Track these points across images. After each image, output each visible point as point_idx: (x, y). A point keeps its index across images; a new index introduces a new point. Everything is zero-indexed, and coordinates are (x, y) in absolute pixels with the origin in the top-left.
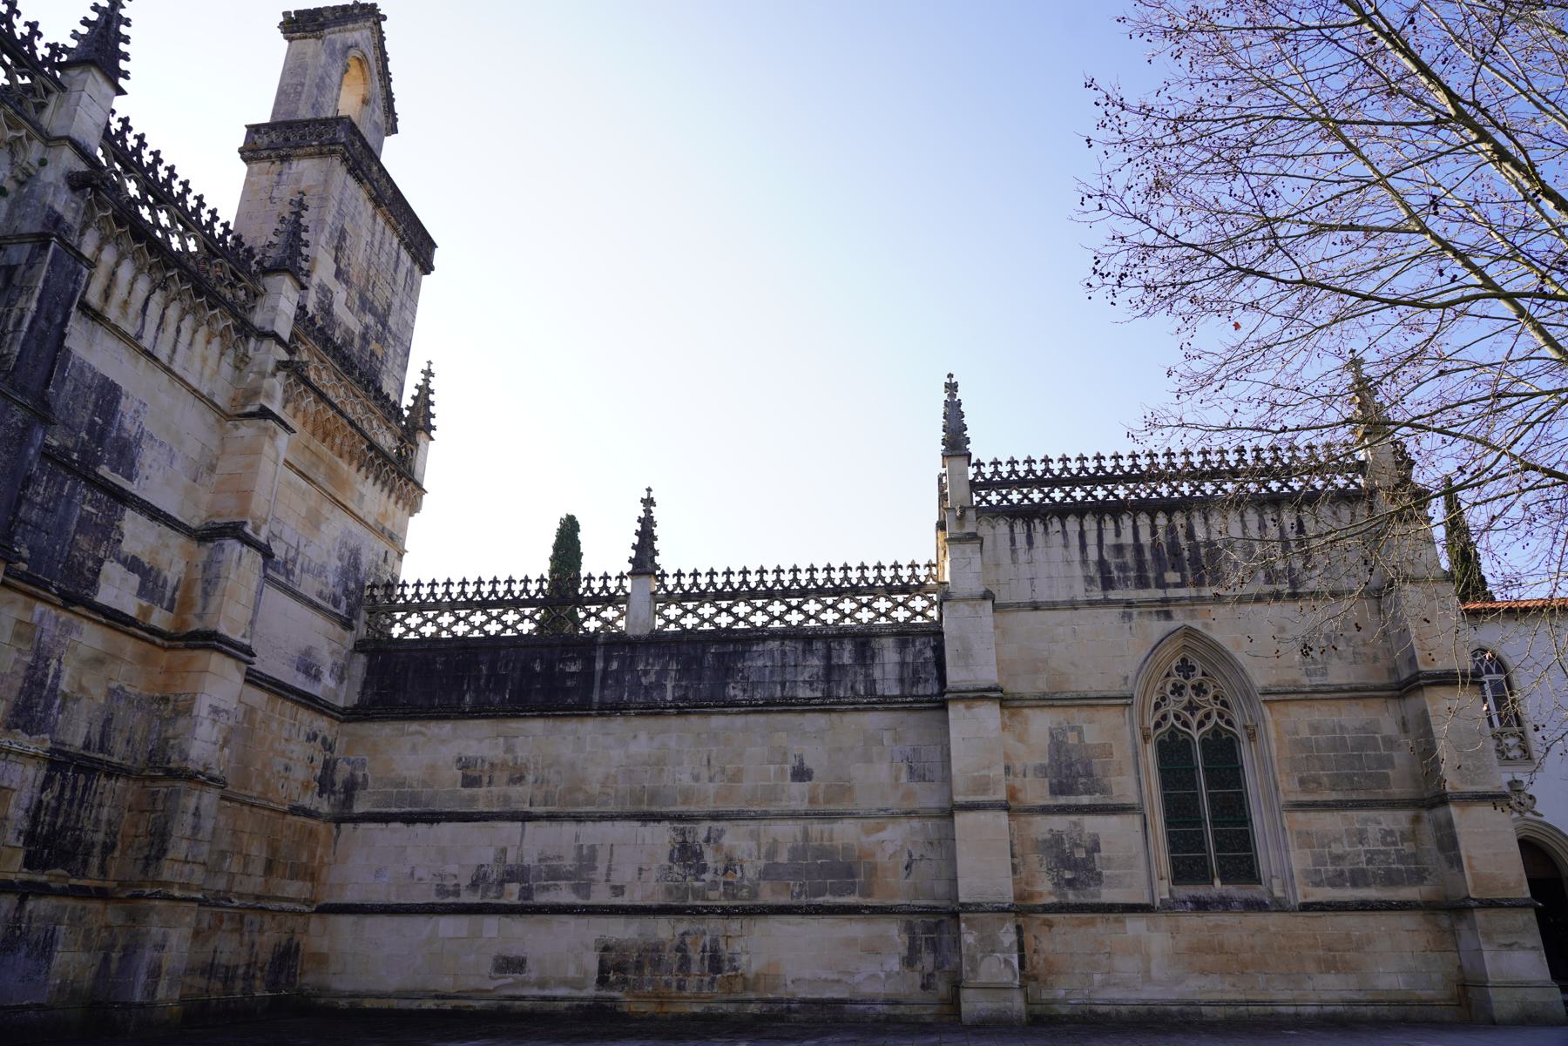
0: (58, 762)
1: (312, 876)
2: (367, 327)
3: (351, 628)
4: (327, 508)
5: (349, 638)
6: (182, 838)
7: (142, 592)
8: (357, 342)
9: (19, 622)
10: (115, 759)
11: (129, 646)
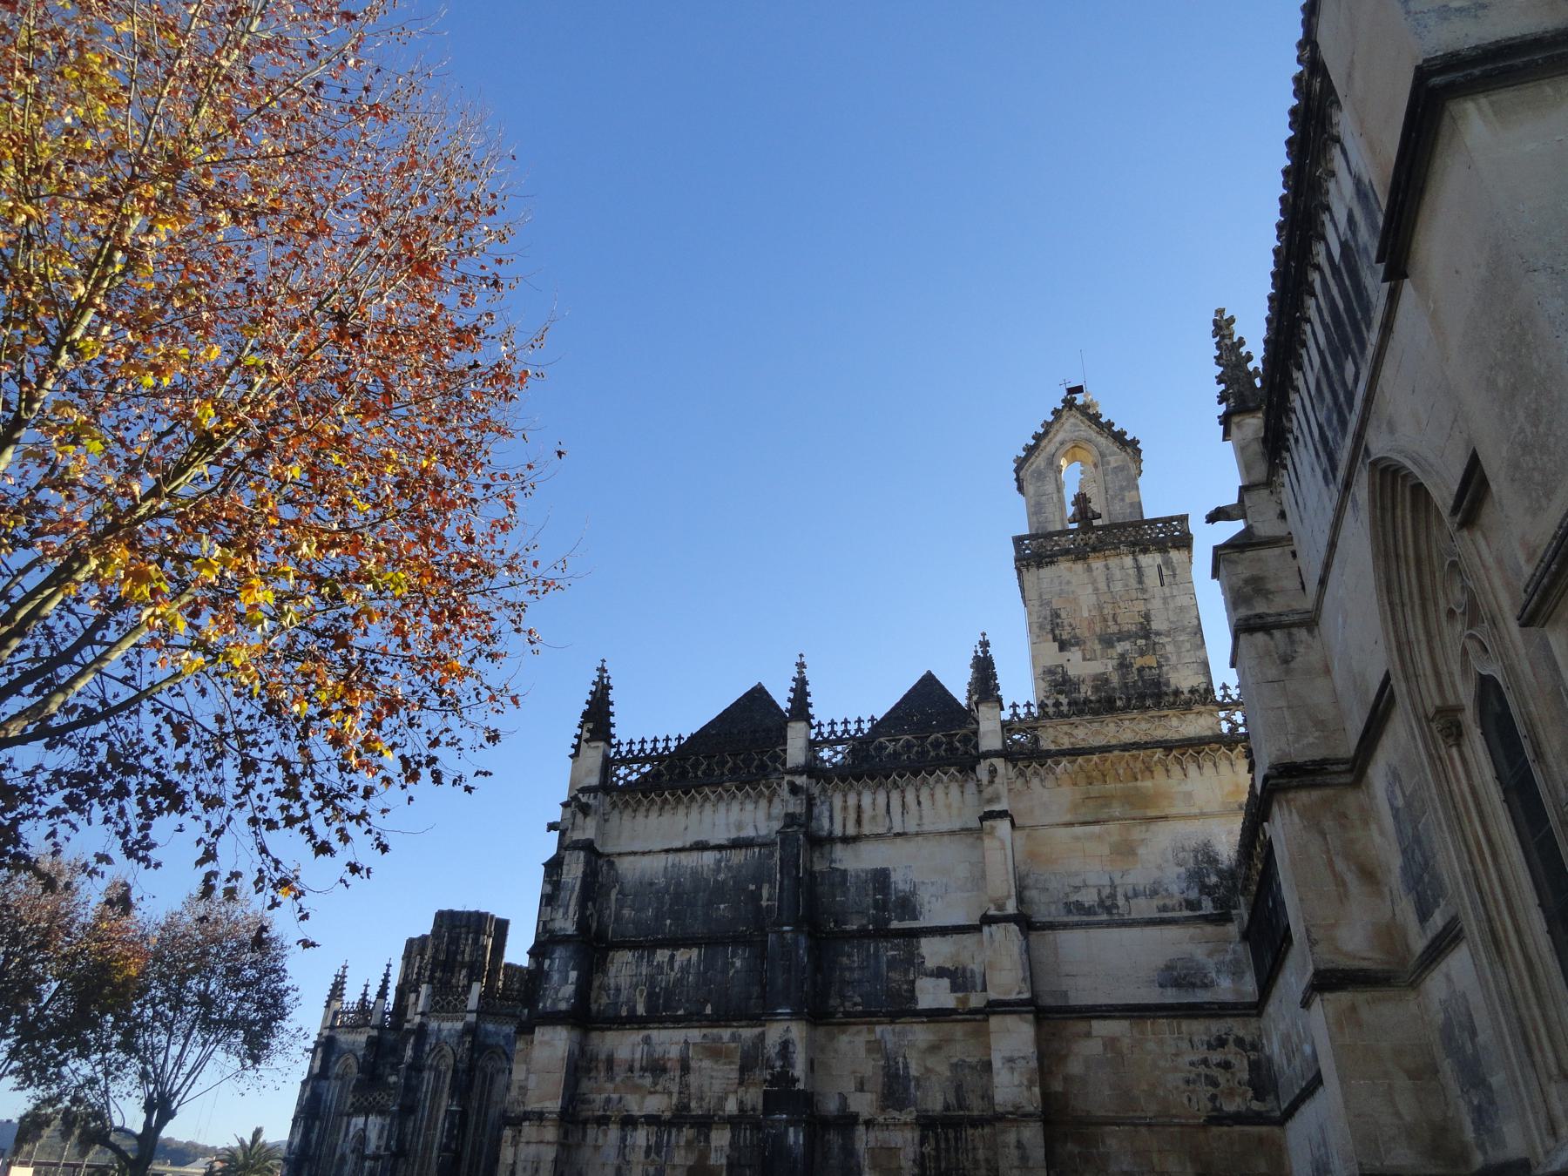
0: (926, 1124)
2: (1122, 656)
3: (1231, 920)
4: (1137, 833)
5: (1233, 929)
7: (955, 988)
8: (1115, 679)
9: (868, 1042)
10: (976, 1113)
11: (959, 1030)
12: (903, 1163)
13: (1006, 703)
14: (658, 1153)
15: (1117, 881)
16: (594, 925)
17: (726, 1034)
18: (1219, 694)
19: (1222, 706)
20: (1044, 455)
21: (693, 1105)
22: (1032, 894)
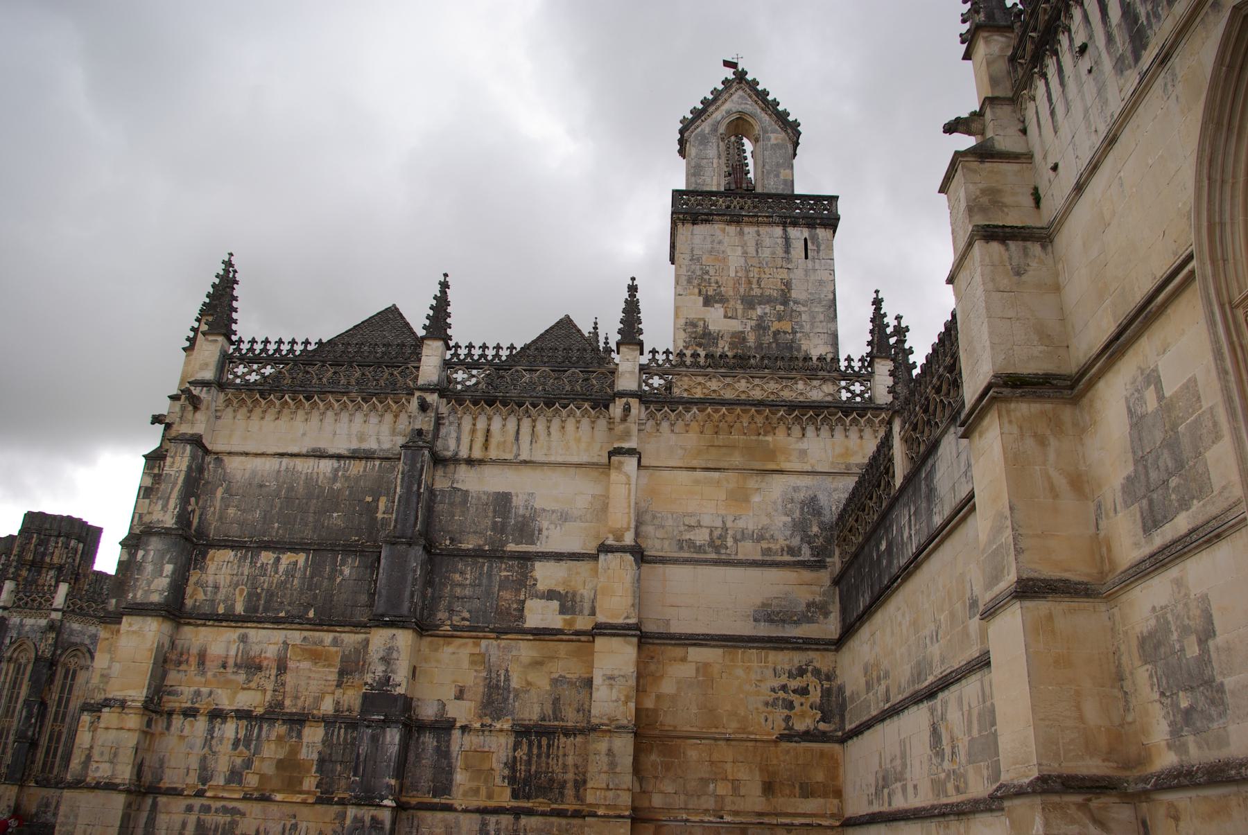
0: (523, 732)
1: (838, 793)
2: (761, 318)
3: (825, 567)
4: (752, 483)
5: (825, 577)
6: (600, 772)
7: (563, 611)
8: (751, 339)
10: (570, 724)
12: (494, 765)
13: (647, 349)
14: (247, 746)
15: (729, 524)
16: (195, 522)
17: (328, 637)
18: (843, 364)
19: (844, 376)
20: (709, 121)
21: (287, 702)
22: (649, 529)
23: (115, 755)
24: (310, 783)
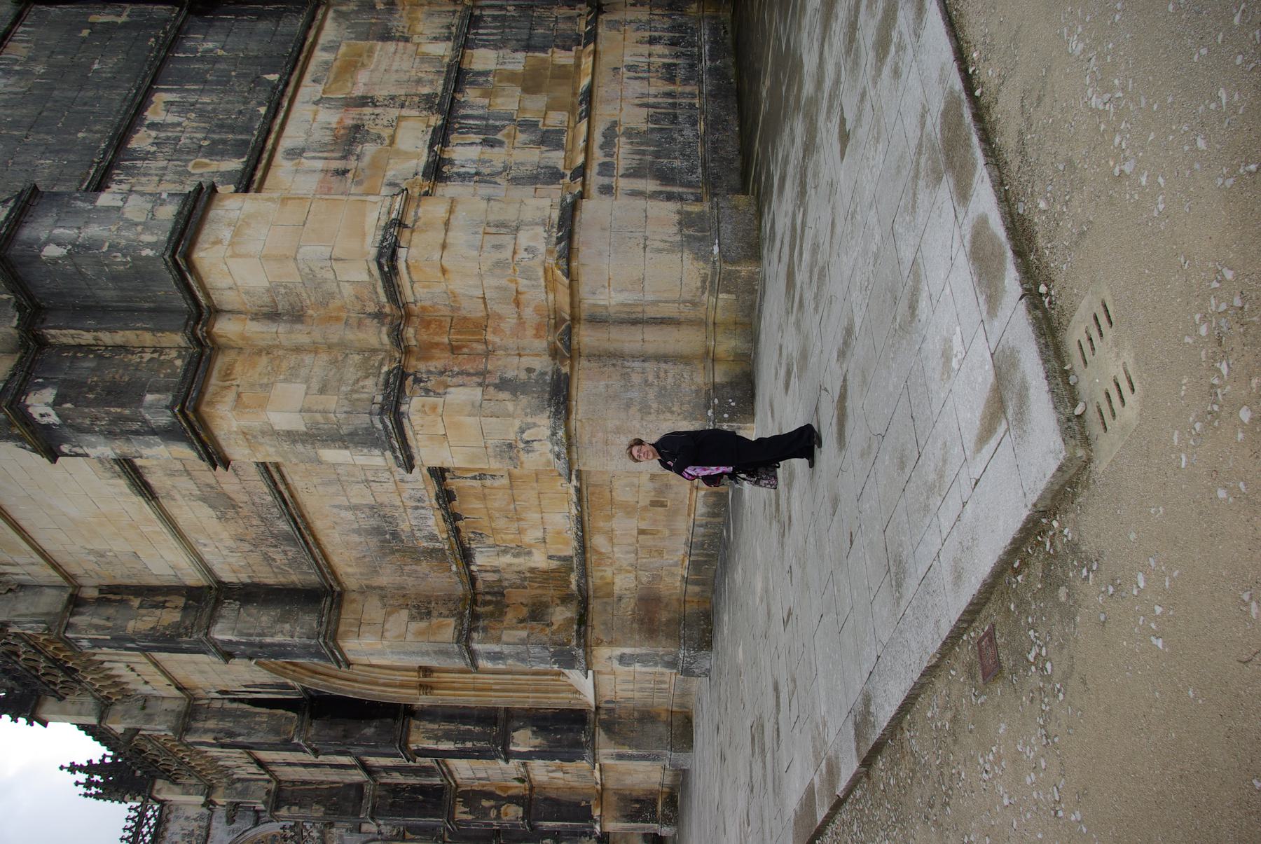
17: (319, 56)
21: (426, 90)
23: (501, 225)
24: (563, 58)
